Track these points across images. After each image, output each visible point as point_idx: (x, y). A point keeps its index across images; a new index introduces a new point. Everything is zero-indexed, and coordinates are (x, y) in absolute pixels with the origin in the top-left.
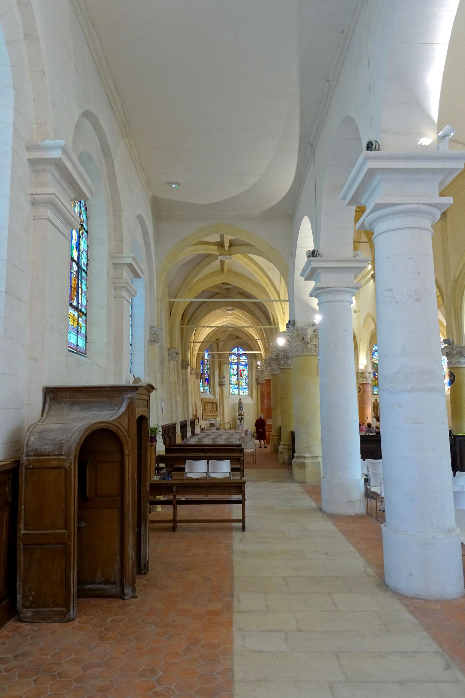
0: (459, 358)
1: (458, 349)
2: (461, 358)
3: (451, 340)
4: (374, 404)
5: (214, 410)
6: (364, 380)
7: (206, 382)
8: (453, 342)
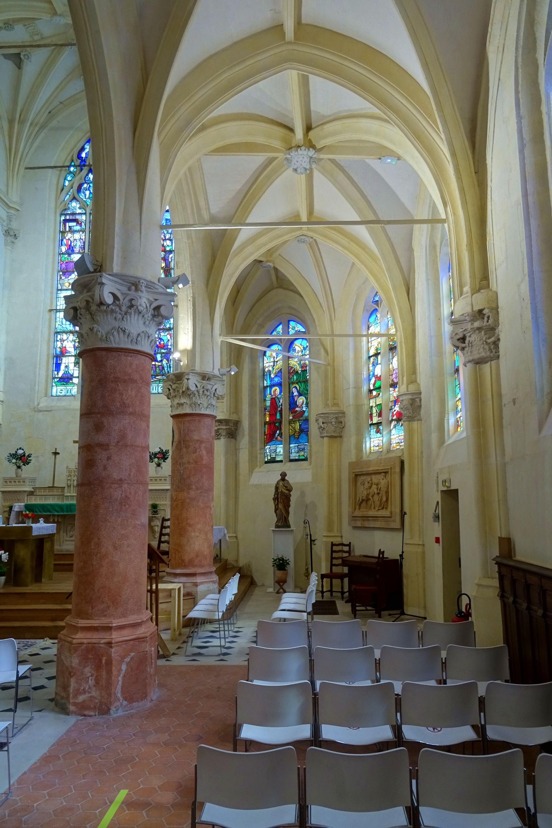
4: (277, 488)
6: (183, 400)
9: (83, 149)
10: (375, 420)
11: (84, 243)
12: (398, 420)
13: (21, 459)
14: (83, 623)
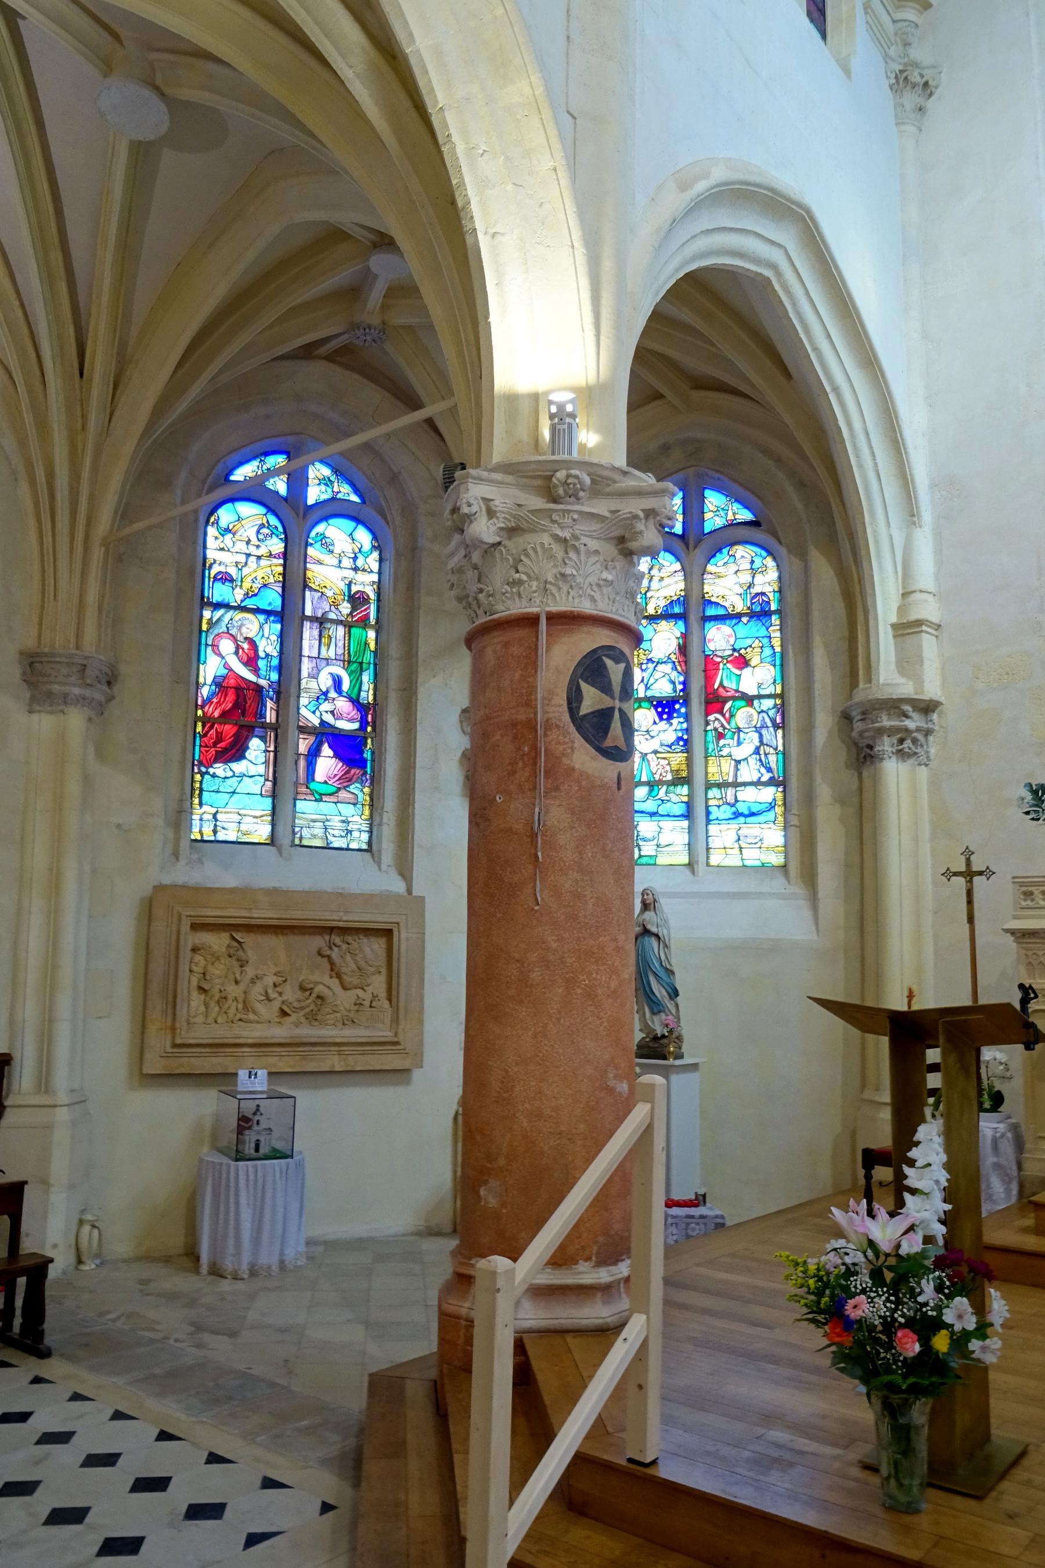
7: (327, 764)
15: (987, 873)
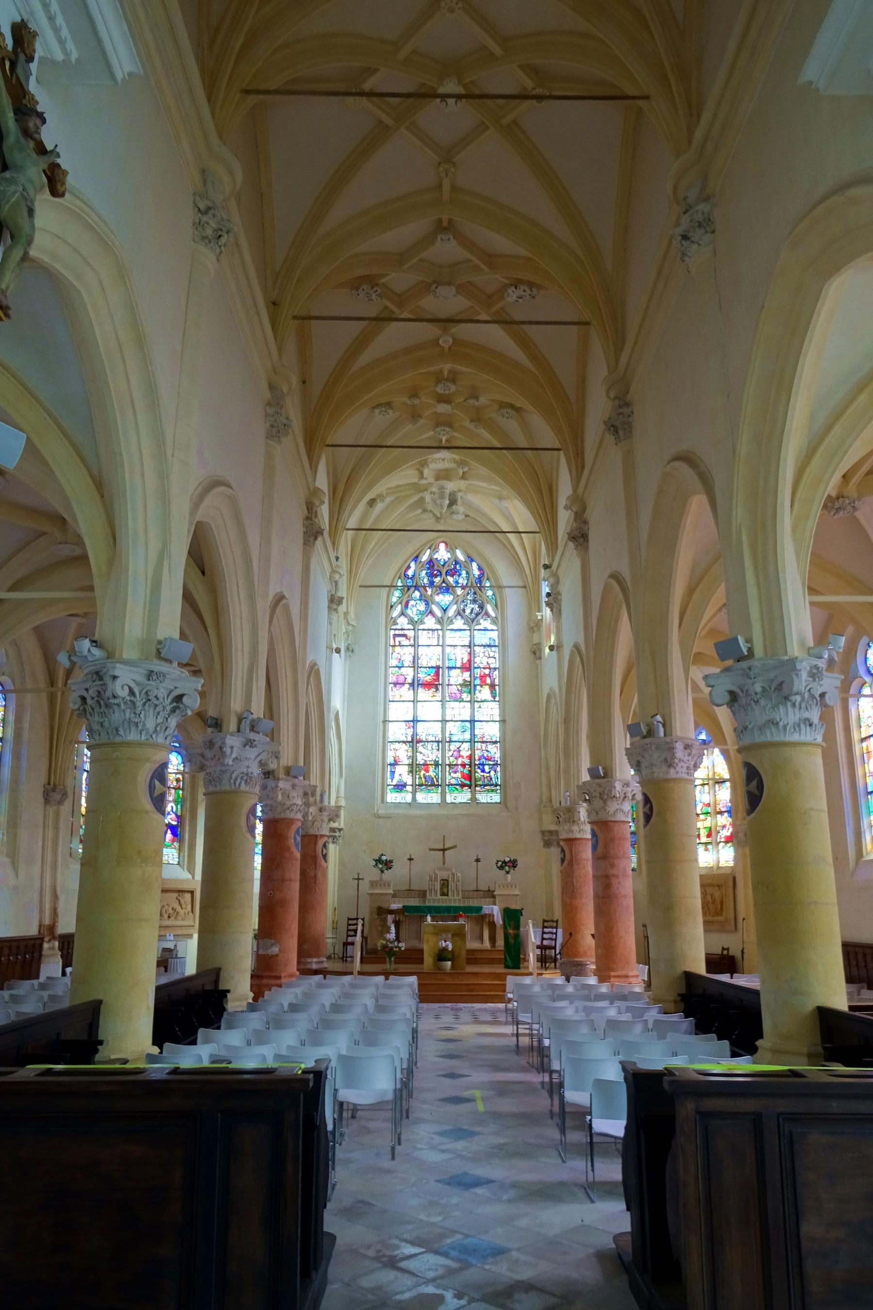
0: (775, 707)
1: (772, 675)
2: (782, 709)
3: (741, 640)
5: (182, 912)
7: (169, 835)
8: (750, 650)
9: (409, 567)
10: (704, 839)
11: (414, 657)
12: (726, 842)
13: (388, 864)
14: (612, 974)
15: (362, 879)
